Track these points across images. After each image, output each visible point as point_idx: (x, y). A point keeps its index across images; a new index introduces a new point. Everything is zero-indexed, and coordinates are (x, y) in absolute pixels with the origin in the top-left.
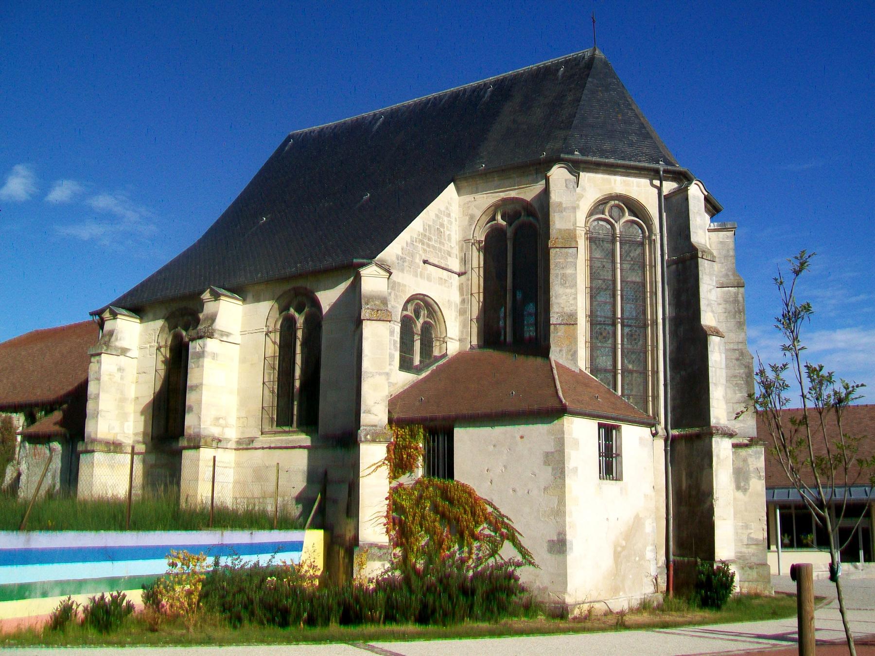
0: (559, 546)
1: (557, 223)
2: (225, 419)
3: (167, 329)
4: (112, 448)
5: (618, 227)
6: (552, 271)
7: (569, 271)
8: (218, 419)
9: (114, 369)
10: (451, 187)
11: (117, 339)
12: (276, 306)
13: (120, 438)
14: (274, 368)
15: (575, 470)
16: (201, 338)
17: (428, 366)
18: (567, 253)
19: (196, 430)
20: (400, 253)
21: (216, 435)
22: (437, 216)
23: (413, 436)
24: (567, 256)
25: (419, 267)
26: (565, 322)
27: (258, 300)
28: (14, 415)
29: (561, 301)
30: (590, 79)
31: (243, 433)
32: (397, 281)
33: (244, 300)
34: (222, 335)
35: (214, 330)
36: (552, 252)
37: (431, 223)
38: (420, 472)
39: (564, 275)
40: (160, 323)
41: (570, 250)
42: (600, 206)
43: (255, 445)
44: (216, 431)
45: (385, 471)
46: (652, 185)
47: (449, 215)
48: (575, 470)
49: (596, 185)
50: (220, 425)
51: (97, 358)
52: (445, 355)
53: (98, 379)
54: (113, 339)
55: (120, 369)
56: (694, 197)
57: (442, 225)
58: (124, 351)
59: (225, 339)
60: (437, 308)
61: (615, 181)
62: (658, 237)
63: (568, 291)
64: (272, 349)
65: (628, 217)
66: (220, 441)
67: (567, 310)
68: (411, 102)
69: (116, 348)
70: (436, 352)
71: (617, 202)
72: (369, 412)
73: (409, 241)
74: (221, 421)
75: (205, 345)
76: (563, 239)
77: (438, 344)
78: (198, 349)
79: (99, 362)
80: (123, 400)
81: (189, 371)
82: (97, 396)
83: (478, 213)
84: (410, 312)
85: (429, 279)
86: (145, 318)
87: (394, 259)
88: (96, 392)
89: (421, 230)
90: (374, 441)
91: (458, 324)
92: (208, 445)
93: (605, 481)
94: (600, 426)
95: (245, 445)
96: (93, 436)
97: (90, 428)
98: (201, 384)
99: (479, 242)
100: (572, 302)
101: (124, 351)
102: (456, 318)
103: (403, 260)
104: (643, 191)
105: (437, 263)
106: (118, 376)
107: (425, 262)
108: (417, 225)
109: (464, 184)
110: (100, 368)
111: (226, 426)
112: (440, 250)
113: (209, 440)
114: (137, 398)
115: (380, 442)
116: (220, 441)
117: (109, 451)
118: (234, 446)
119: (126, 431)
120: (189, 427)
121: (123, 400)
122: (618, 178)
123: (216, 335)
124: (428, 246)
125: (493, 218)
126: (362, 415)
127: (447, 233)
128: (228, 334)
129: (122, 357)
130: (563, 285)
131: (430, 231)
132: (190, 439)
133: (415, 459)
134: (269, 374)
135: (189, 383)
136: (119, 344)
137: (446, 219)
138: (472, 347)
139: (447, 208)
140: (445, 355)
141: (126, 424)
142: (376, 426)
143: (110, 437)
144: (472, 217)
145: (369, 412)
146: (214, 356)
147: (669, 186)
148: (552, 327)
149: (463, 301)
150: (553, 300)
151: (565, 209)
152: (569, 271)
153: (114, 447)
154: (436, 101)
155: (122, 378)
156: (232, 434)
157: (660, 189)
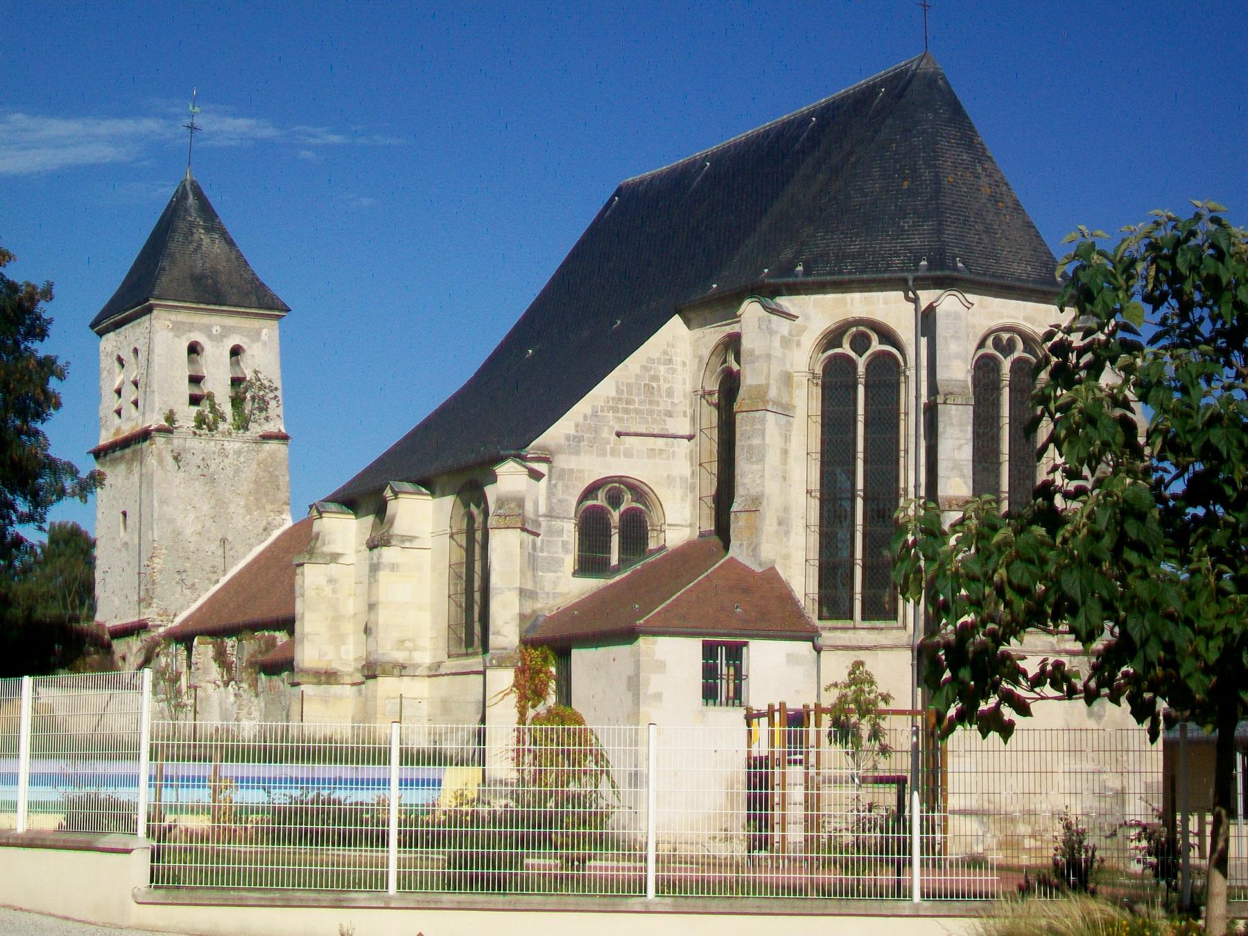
0: (635, 779)
1: (748, 377)
2: (413, 640)
4: (323, 678)
5: (861, 363)
6: (737, 443)
7: (756, 441)
8: (403, 642)
9: (322, 581)
10: (676, 321)
11: (324, 544)
12: (458, 501)
13: (335, 666)
14: (461, 577)
15: (658, 696)
17: (626, 568)
18: (754, 418)
20: (572, 432)
21: (401, 661)
22: (644, 368)
23: (545, 659)
24: (753, 420)
25: (608, 443)
26: (747, 508)
27: (443, 495)
28: (277, 634)
29: (747, 481)
30: (889, 121)
31: (435, 657)
32: (566, 467)
33: (433, 494)
34: (403, 541)
35: (391, 536)
36: (739, 417)
37: (633, 380)
38: (552, 699)
39: (750, 447)
41: (758, 414)
42: (832, 338)
43: (442, 671)
44: (400, 656)
45: (513, 698)
46: (907, 298)
47: (670, 361)
48: (658, 696)
49: (818, 312)
50: (406, 649)
52: (663, 547)
53: (303, 596)
54: (319, 543)
56: (948, 314)
57: (655, 378)
58: (334, 558)
59: (407, 544)
60: (646, 489)
61: (852, 300)
62: (913, 371)
63: (755, 467)
64: (460, 555)
65: (876, 346)
66: (404, 667)
67: (753, 492)
68: (741, 136)
69: (324, 555)
70: (652, 545)
71: (861, 328)
72: (498, 633)
73: (589, 412)
74: (407, 644)
75: (380, 556)
76: (750, 398)
77: (655, 534)
79: (303, 574)
80: (337, 618)
83: (706, 353)
84: (600, 500)
85: (628, 454)
87: (562, 441)
89: (613, 394)
90: (499, 666)
91: (688, 505)
92: (386, 673)
93: (730, 708)
94: (705, 644)
95: (435, 672)
99: (711, 393)
100: (759, 481)
101: (334, 558)
102: (683, 499)
103: (578, 439)
104: (891, 308)
105: (644, 431)
106: (328, 589)
107: (619, 435)
108: (605, 389)
109: (692, 315)
111: (415, 649)
112: (651, 412)
113: (388, 667)
115: (507, 667)
116: (404, 667)
117: (319, 683)
118: (426, 672)
119: (344, 657)
121: (337, 618)
122: (857, 296)
123: (393, 542)
124: (626, 411)
125: (725, 361)
126: (491, 637)
127: (665, 386)
128: (412, 539)
129: (333, 565)
130: (749, 460)
131: (630, 392)
133: (547, 685)
134: (456, 585)
136: (326, 549)
137: (662, 368)
138: (701, 535)
139: (666, 353)
140: (663, 547)
141: (343, 648)
142: (505, 649)
143: (321, 665)
144: (701, 358)
145: (498, 633)
146: (393, 567)
147: (926, 297)
148: (732, 516)
149: (693, 473)
150: (738, 479)
151: (758, 357)
152: (756, 441)
153: (328, 677)
154: (767, 133)
155: (334, 591)
156: (425, 658)
157: (916, 301)
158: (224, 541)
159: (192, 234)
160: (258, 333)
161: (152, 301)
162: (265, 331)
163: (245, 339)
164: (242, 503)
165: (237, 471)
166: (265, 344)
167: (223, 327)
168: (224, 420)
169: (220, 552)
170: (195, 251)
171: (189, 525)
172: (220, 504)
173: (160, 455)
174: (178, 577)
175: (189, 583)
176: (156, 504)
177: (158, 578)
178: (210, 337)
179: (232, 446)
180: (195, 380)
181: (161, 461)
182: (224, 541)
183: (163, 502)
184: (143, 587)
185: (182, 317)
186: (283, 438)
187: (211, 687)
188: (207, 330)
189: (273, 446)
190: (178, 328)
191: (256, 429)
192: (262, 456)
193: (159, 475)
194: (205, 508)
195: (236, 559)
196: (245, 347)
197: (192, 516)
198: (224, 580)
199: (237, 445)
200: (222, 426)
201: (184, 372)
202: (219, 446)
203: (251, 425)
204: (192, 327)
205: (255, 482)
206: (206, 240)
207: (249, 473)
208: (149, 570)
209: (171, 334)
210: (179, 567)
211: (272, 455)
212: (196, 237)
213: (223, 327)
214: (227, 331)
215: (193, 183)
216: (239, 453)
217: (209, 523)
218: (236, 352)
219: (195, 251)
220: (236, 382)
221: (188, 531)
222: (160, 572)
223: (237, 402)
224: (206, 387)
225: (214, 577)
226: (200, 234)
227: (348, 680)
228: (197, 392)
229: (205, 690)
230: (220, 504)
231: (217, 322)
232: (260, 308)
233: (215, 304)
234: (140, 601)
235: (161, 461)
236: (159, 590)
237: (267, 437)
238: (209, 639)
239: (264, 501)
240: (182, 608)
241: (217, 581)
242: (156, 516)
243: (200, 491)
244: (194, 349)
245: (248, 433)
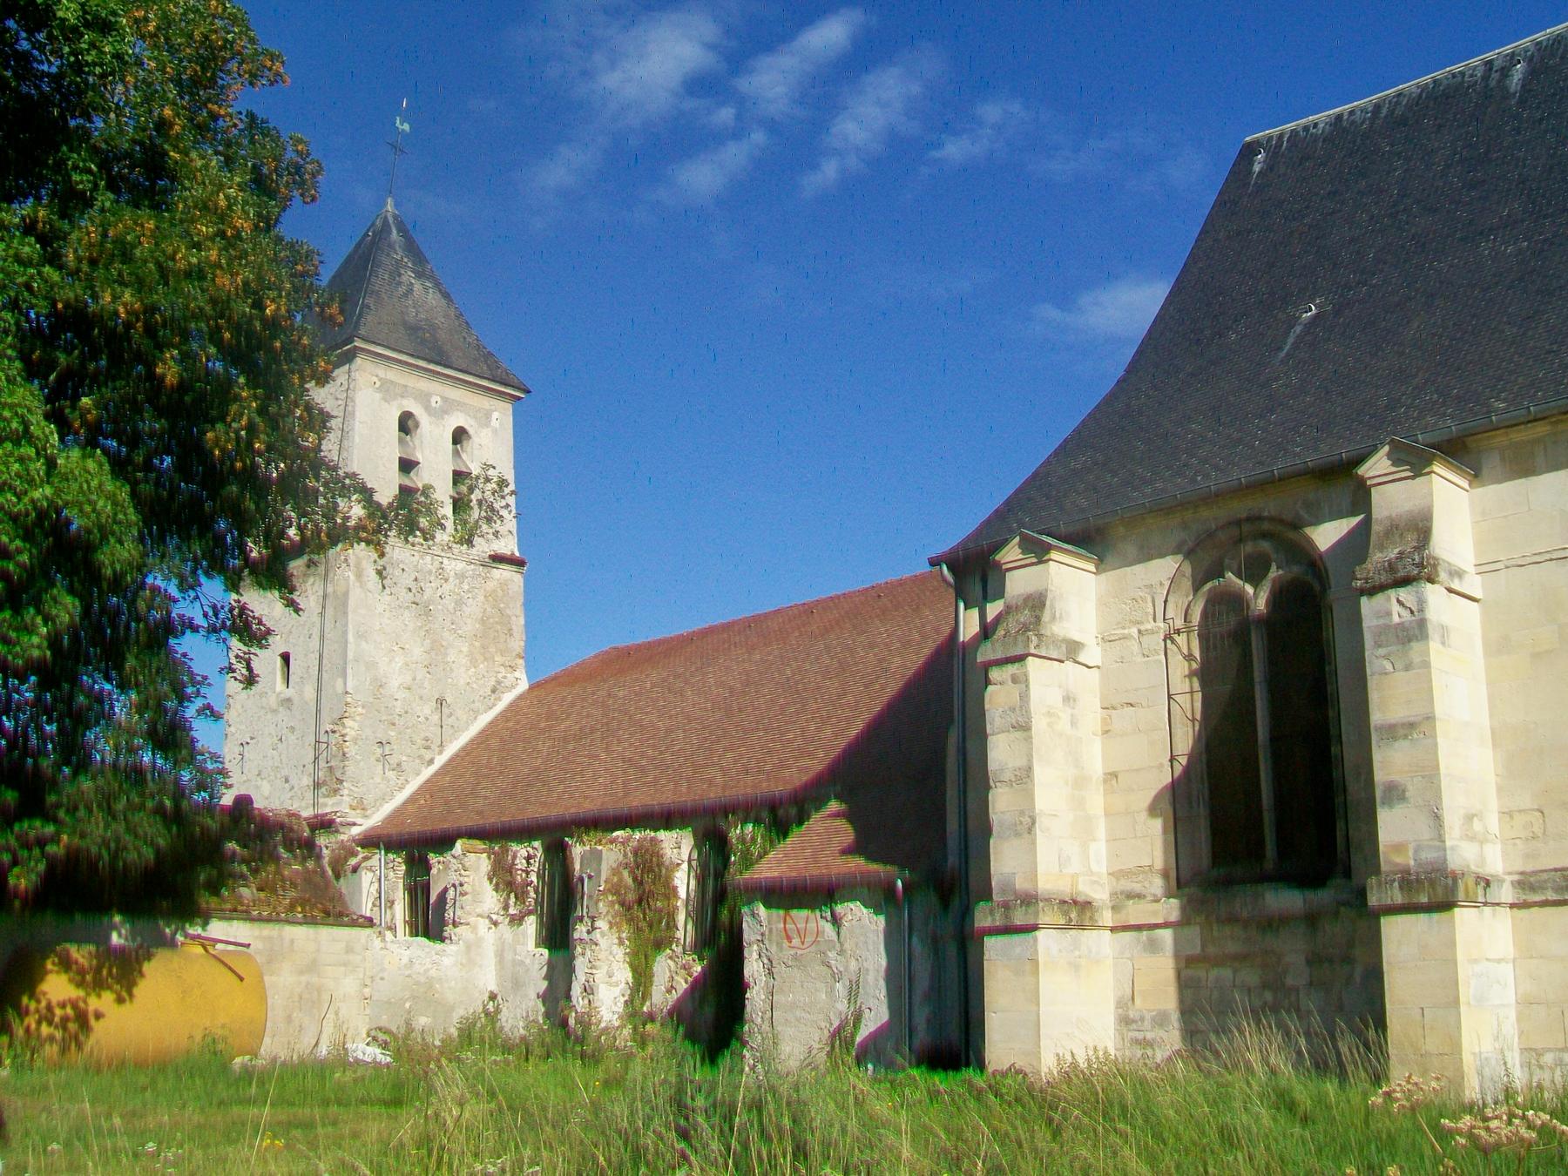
3: (1187, 584)
9: (1055, 698)
13: (1087, 890)
16: (1405, 582)
19: (1428, 855)
28: (662, 835)
35: (1435, 564)
40: (1165, 568)
51: (1011, 669)
53: (1024, 727)
54: (1046, 617)
55: (1068, 699)
58: (1072, 650)
69: (1056, 641)
75: (1422, 603)
78: (1397, 615)
79: (1021, 680)
80: (1080, 782)
81: (1372, 683)
82: (1025, 776)
86: (1109, 559)
88: (1021, 762)
96: (1021, 884)
97: (1005, 862)
98: (1430, 718)
110: (1024, 697)
114: (1115, 775)
119: (1094, 868)
120: (1399, 848)
129: (1069, 664)
132: (1408, 881)
135: (1376, 717)
153: (1078, 912)
158: (441, 702)
159: (400, 275)
160: (488, 415)
161: (358, 343)
162: (495, 415)
163: (472, 422)
164: (465, 649)
165: (459, 603)
166: (495, 431)
167: (445, 399)
168: (443, 527)
169: (436, 718)
170: (406, 295)
171: (396, 676)
172: (437, 648)
173: (358, 565)
174: (379, 751)
175: (393, 760)
176: (351, 638)
177: (351, 749)
178: (427, 408)
179: (454, 566)
180: (407, 466)
181: (359, 575)
182: (441, 702)
183: (361, 636)
184: (322, 764)
185: (393, 374)
186: (518, 563)
187: (483, 924)
188: (424, 398)
189: (504, 573)
190: (388, 390)
191: (483, 547)
192: (491, 585)
193: (355, 595)
194: (418, 652)
195: (457, 730)
196: (471, 431)
197: (399, 661)
198: (440, 760)
199: (460, 566)
200: (442, 537)
201: (394, 454)
202: (436, 564)
203: (477, 540)
204: (404, 392)
205: (482, 622)
206: (417, 286)
207: (474, 608)
208: (334, 738)
209: (378, 396)
210: (381, 736)
211: (504, 585)
212: (404, 279)
213: (445, 399)
214: (448, 407)
215: (395, 217)
216: (461, 576)
217: (422, 673)
218: (459, 436)
219: (406, 295)
220: (459, 476)
221: (394, 683)
222: (355, 740)
223: (460, 505)
224: (418, 479)
225: (428, 755)
226: (408, 276)
227: (1107, 918)
228: (407, 482)
229: (475, 929)
230: (437, 648)
231: (439, 391)
232: (493, 380)
233: (430, 361)
234: (317, 785)
235: (359, 575)
236: (351, 769)
237: (498, 559)
238: (479, 844)
239: (492, 650)
240: (383, 799)
241: (431, 762)
242: (350, 655)
243: (411, 626)
244: (406, 424)
245: (474, 551)
